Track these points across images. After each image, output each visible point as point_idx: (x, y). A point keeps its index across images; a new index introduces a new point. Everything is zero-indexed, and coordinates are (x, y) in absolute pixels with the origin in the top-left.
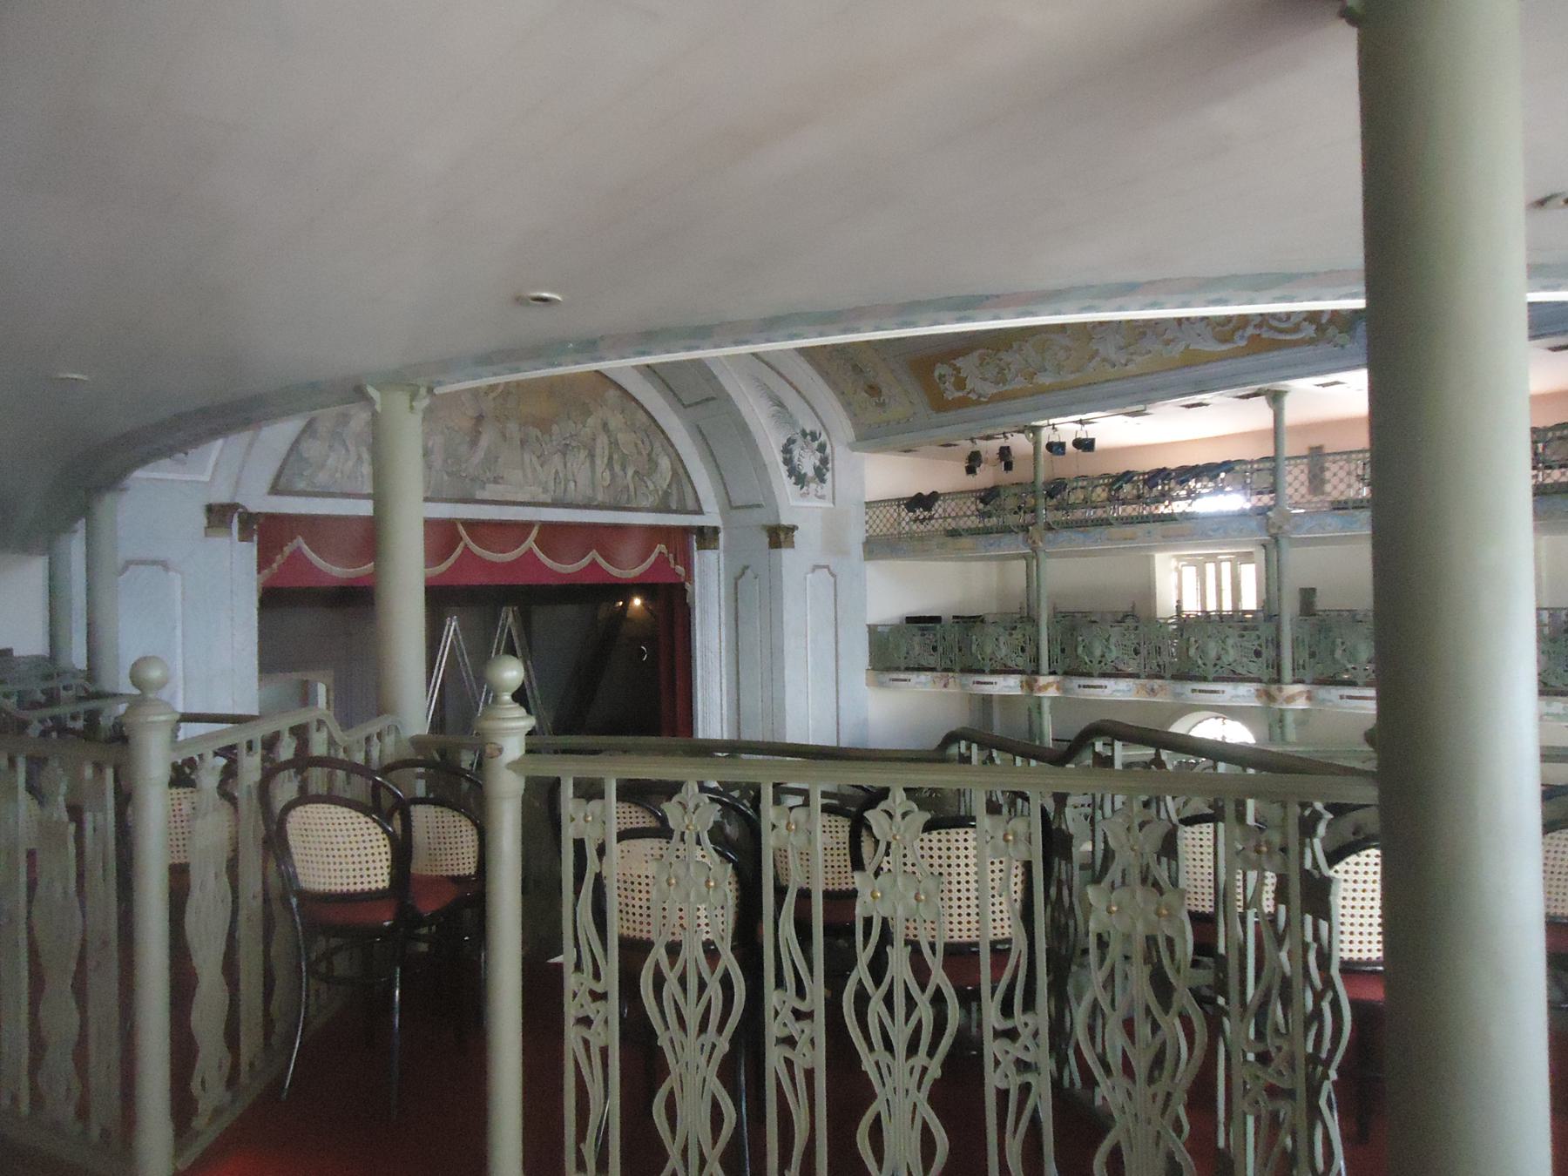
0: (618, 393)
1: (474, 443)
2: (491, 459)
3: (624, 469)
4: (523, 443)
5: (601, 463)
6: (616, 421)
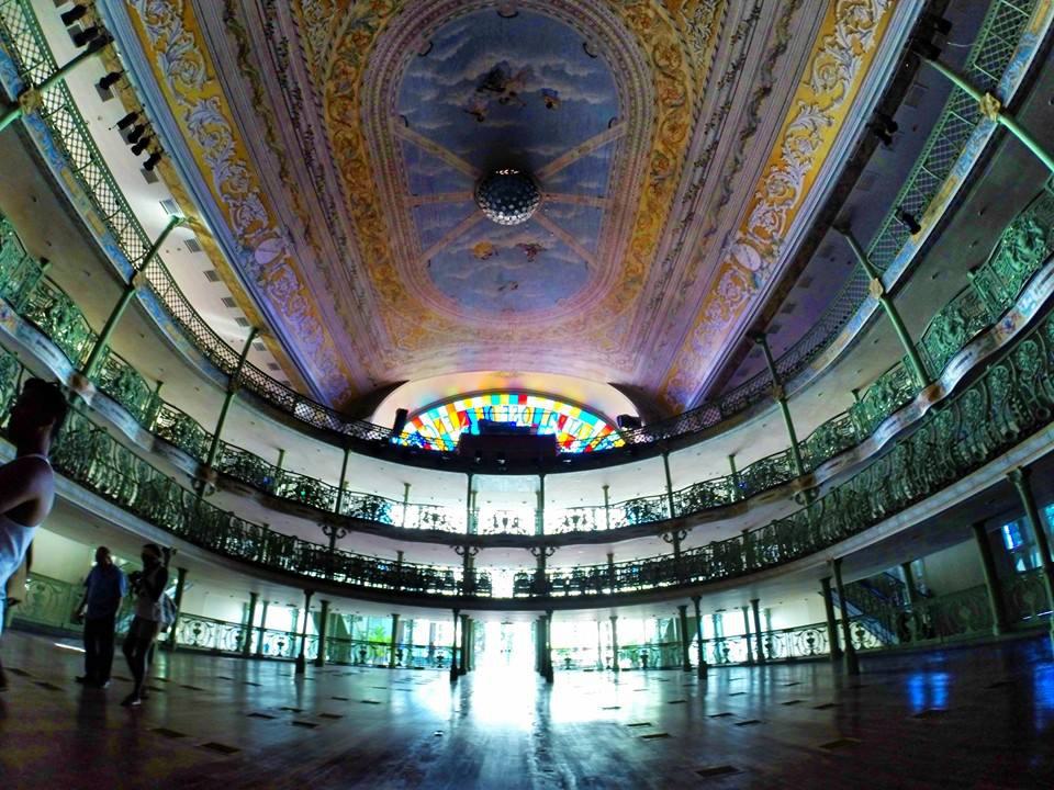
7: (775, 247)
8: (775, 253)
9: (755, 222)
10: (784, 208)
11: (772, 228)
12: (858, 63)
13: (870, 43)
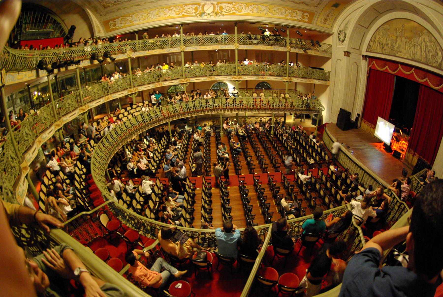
0: (427, 31)
1: (396, 42)
2: (399, 46)
3: (429, 52)
4: (406, 43)
5: (423, 50)
6: (427, 39)
7: (220, 14)
8: (218, 15)
9: (223, 5)
10: (234, 11)
11: (225, 10)
12: (283, 16)
13: (288, 18)
